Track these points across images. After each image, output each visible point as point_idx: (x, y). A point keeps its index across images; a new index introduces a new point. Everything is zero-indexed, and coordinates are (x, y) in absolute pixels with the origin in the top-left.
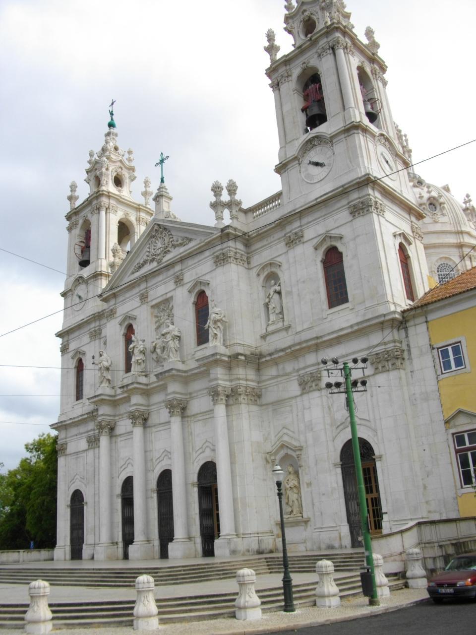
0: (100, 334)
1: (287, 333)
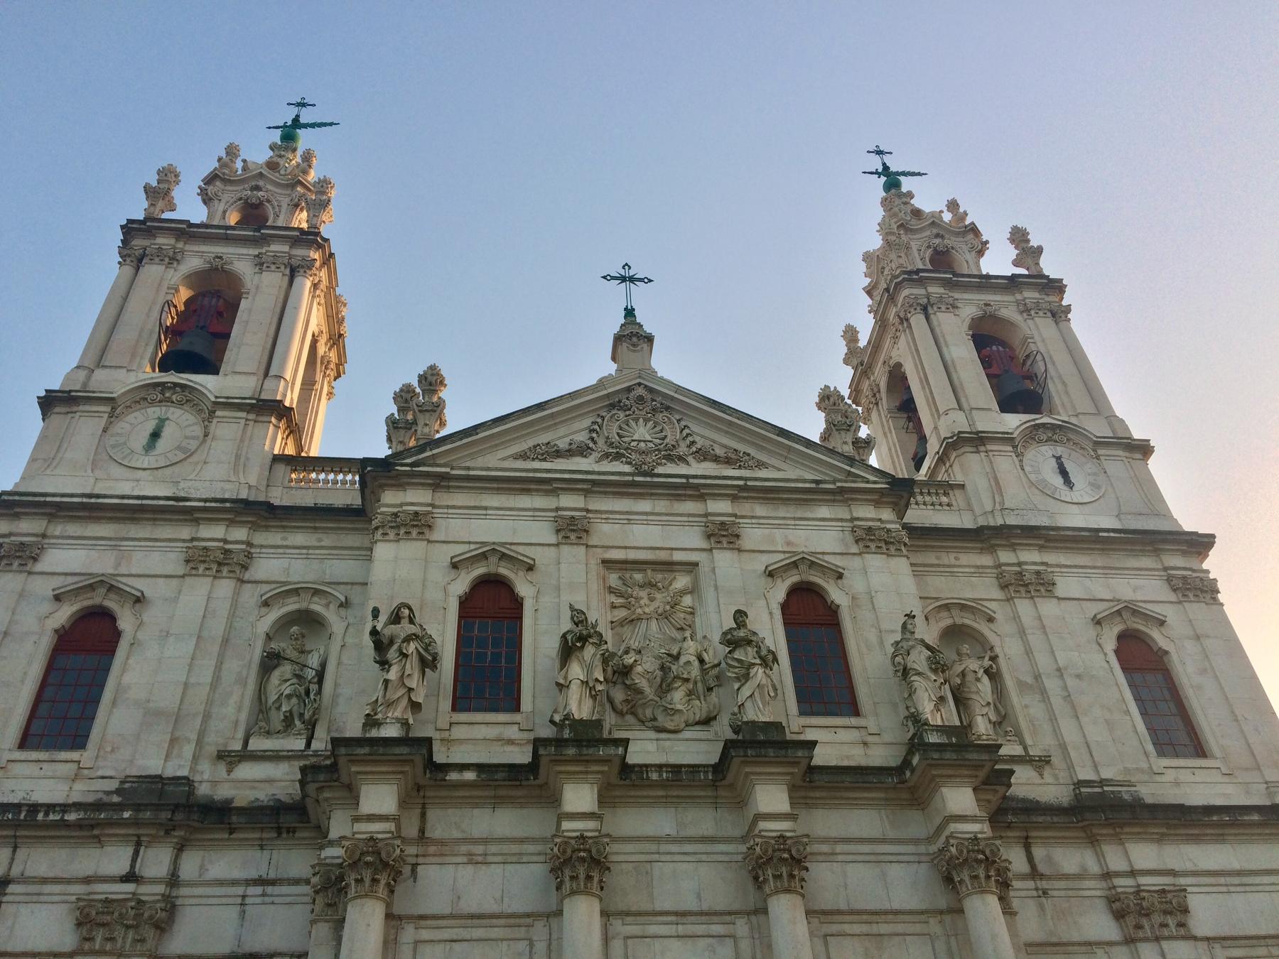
0: (245, 567)
1: (1041, 775)
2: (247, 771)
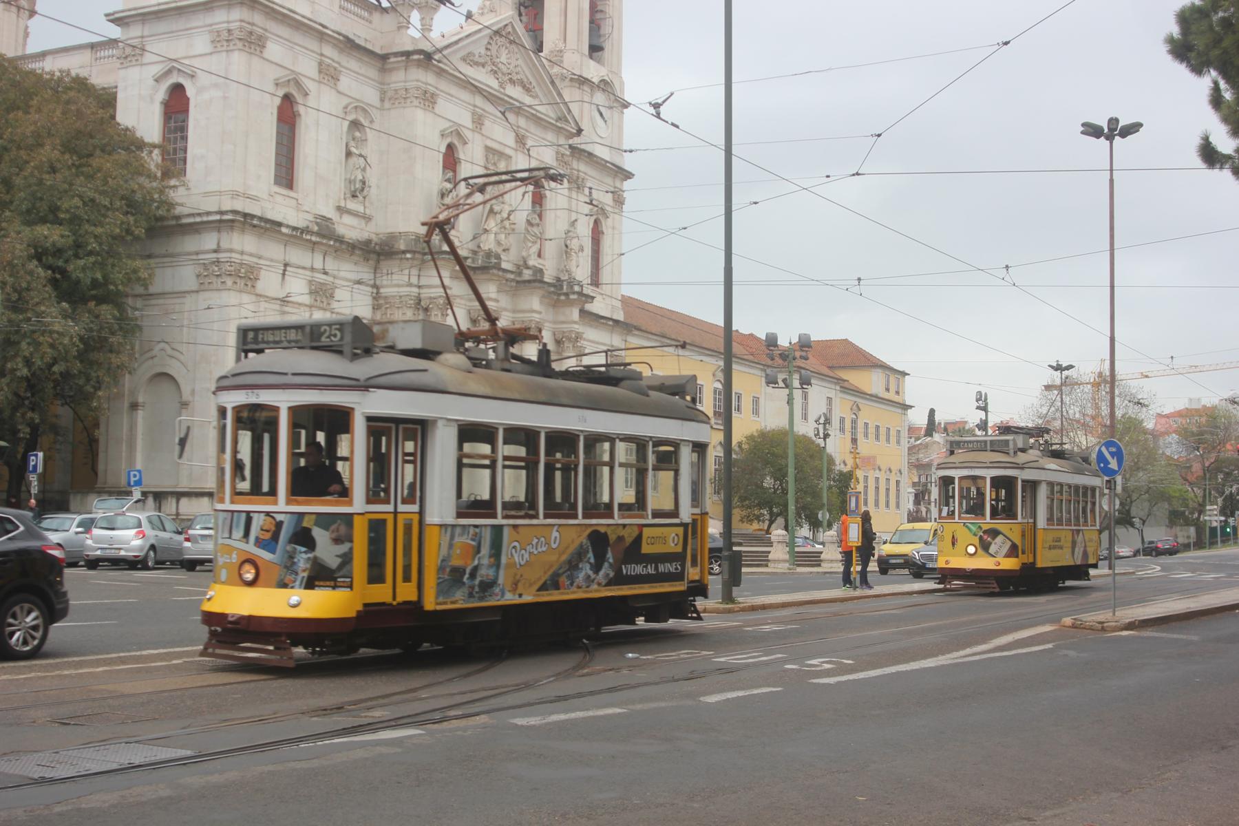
2: (347, 219)
